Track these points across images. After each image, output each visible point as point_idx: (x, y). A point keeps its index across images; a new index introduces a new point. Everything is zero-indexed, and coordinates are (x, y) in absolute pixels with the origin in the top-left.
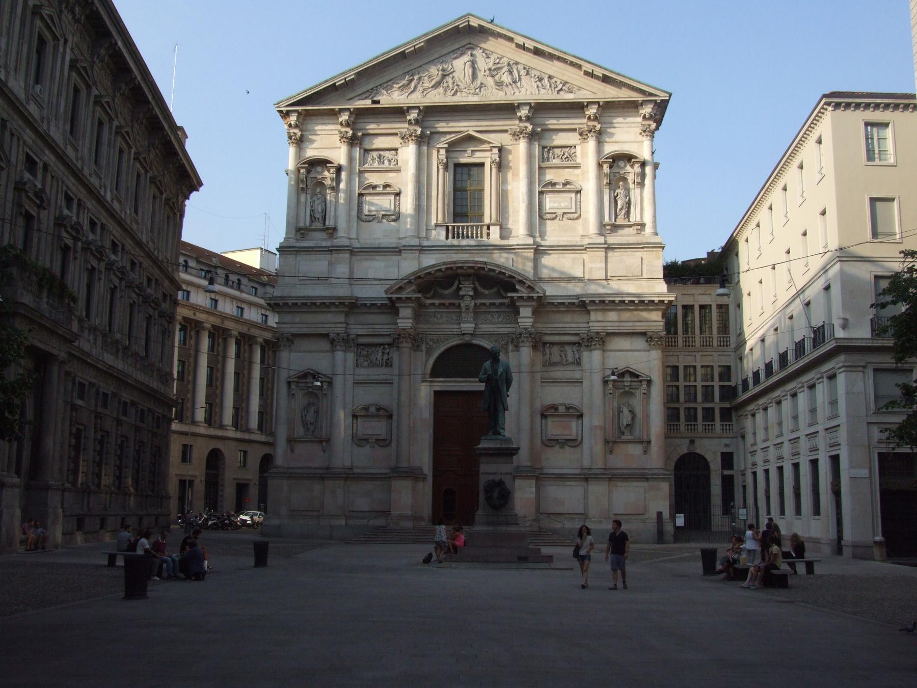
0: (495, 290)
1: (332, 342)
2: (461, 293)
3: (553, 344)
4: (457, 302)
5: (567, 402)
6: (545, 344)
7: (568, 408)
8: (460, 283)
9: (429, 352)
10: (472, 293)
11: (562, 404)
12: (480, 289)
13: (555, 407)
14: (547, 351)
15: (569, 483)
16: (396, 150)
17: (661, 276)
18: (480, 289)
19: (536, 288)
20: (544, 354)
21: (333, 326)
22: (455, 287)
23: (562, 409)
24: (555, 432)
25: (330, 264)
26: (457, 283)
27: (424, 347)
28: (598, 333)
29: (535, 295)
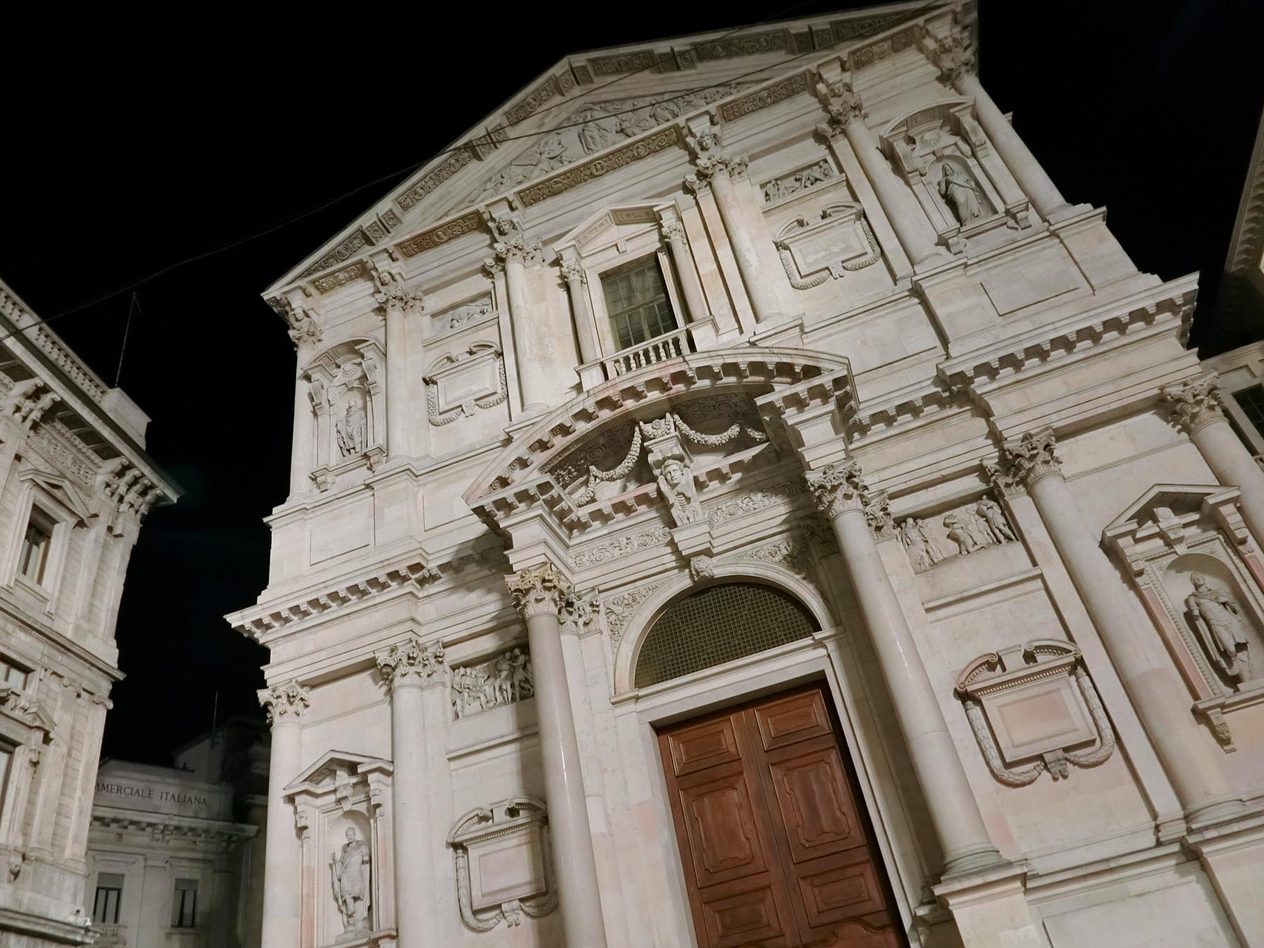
0: (734, 431)
1: (385, 674)
2: (651, 458)
3: (918, 516)
4: (650, 489)
5: (1026, 641)
6: (900, 522)
7: (1029, 657)
8: (644, 438)
9: (616, 630)
10: (678, 450)
11: (1011, 650)
12: (693, 434)
13: (993, 663)
14: (914, 534)
15: (1135, 887)
16: (487, 294)
17: (1132, 267)
18: (693, 434)
19: (822, 365)
20: (908, 543)
21: (385, 634)
22: (635, 450)
23: (1015, 662)
24: (1020, 737)
25: (375, 513)
26: (637, 439)
27: (601, 621)
28: (1027, 437)
29: (825, 380)
